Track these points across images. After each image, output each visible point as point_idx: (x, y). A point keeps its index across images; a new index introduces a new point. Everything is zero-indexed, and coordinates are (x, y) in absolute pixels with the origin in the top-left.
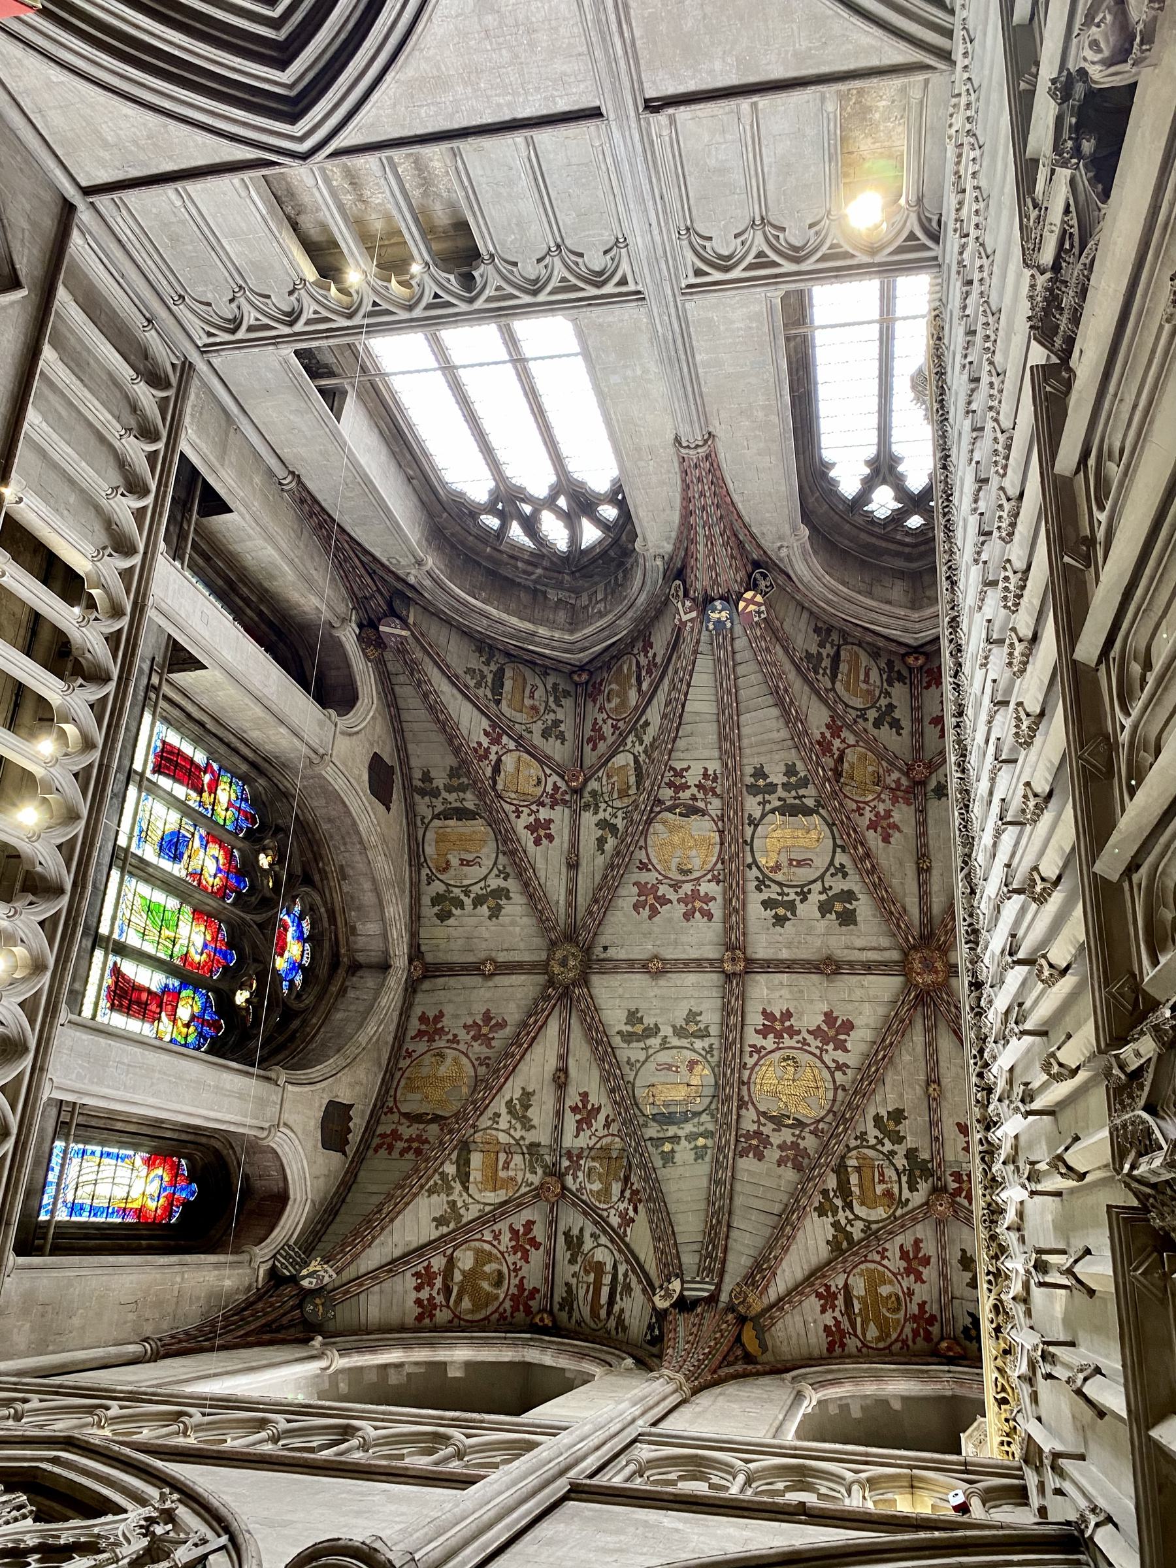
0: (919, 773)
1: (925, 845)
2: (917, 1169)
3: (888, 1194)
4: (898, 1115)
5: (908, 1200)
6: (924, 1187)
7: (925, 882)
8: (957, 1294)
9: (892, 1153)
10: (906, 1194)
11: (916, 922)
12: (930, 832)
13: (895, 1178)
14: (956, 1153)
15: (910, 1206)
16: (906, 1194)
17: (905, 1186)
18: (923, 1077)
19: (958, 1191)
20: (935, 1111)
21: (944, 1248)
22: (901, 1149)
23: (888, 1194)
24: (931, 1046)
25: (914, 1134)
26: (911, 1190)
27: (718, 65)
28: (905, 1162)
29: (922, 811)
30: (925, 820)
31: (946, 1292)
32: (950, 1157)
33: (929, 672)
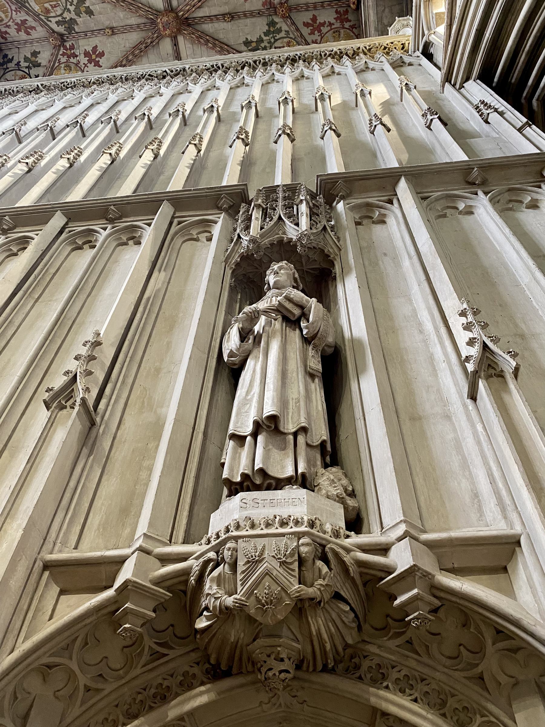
0: (280, 11)
1: (239, 17)
2: (70, 24)
3: (47, 11)
4: (89, 12)
5: (51, 21)
6: (61, 29)
7: (217, 19)
8: (21, 50)
9: (69, 11)
10: (54, 20)
11: (195, 15)
12: (248, 20)
13: (58, 13)
14: (83, 46)
15: (49, 23)
16: (54, 20)
17: (57, 19)
18: (115, 25)
19: (65, 48)
20: (99, 33)
21: (37, 42)
22: (73, 16)
23: (47, 11)
24: (128, 29)
25: (84, 22)
26: (56, 22)
28: (68, 18)
29: (259, 14)
30: (254, 16)
31: (20, 44)
32: (82, 42)
33: (347, 12)
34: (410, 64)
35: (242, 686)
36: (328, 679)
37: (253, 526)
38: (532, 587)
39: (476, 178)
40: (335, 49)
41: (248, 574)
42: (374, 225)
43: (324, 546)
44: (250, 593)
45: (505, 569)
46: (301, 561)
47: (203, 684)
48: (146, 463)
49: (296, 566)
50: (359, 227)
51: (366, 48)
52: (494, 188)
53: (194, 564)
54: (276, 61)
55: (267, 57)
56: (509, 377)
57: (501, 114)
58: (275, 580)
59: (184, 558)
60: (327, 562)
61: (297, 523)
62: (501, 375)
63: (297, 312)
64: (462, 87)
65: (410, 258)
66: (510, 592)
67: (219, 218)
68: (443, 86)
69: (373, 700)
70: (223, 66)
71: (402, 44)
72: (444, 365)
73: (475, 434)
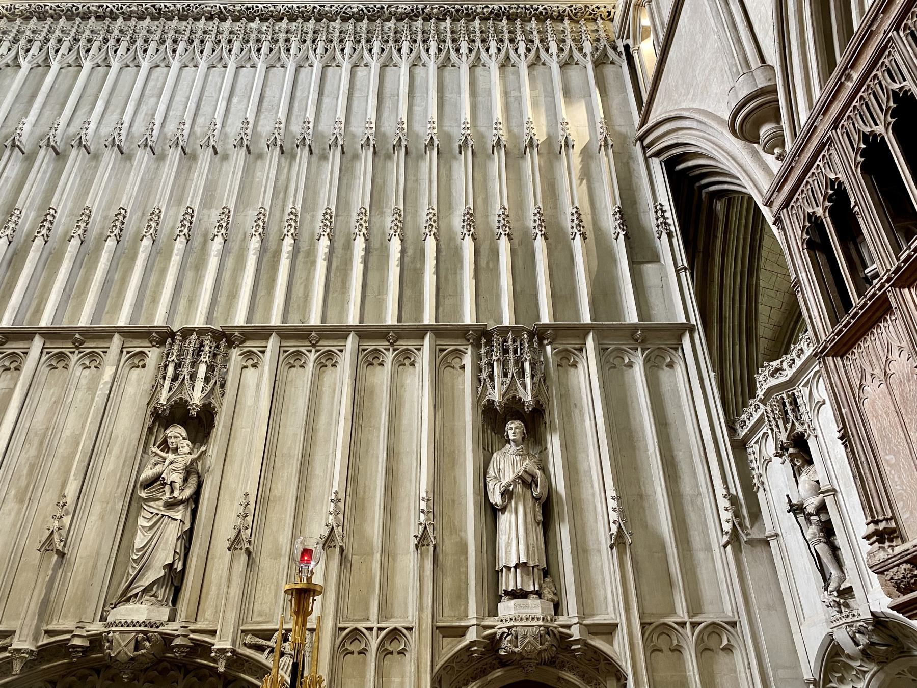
27: (686, 20)
34: (612, 63)
35: (511, 669)
36: (545, 667)
37: (521, 619)
38: (619, 644)
39: (639, 338)
40: (541, 8)
41: (522, 642)
42: (569, 368)
43: (548, 629)
44: (523, 649)
45: (611, 634)
46: (541, 636)
47: (498, 668)
48: (463, 569)
49: (539, 639)
50: (560, 368)
51: (571, 10)
52: (649, 346)
53: (499, 632)
54: (480, 14)
55: (470, 6)
56: (627, 547)
57: (670, 235)
58: (532, 645)
59: (493, 627)
60: (549, 635)
61: (538, 619)
62: (624, 543)
63: (530, 480)
64: (650, 157)
65: (590, 420)
66: (611, 644)
67: (467, 349)
68: (636, 141)
69: (560, 675)
70: (423, 12)
71: (608, 12)
72: (601, 518)
73: (610, 567)
